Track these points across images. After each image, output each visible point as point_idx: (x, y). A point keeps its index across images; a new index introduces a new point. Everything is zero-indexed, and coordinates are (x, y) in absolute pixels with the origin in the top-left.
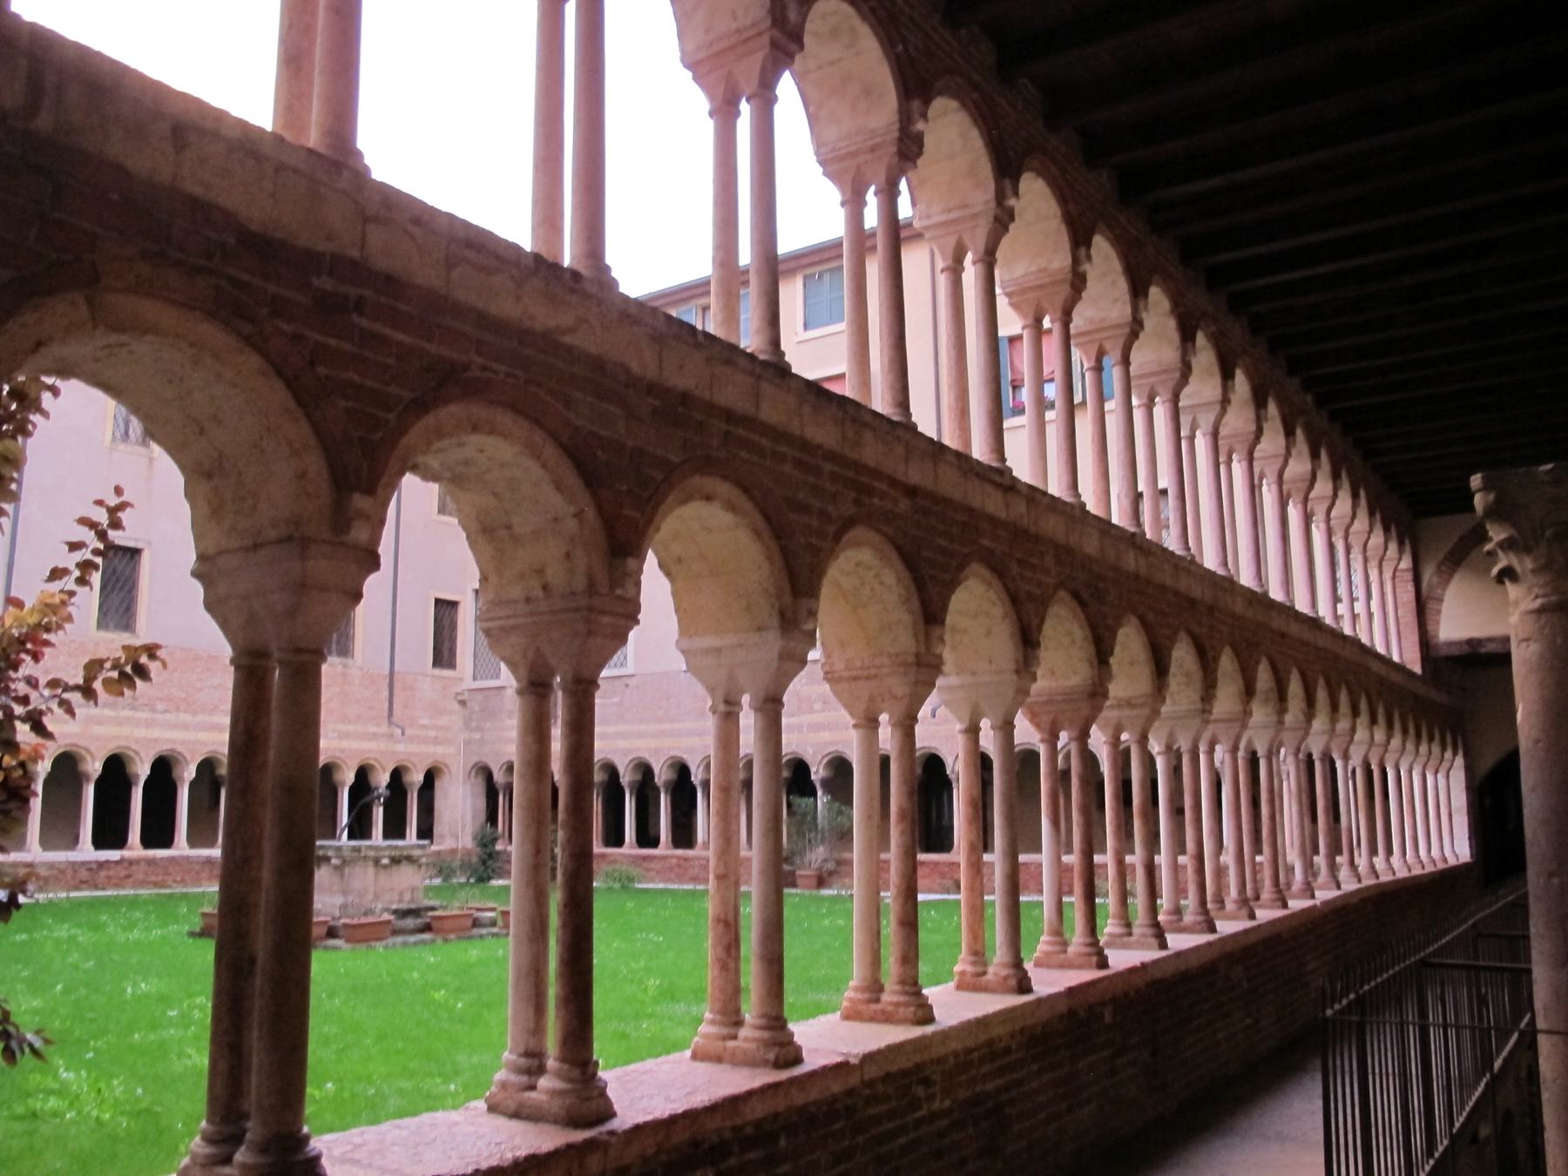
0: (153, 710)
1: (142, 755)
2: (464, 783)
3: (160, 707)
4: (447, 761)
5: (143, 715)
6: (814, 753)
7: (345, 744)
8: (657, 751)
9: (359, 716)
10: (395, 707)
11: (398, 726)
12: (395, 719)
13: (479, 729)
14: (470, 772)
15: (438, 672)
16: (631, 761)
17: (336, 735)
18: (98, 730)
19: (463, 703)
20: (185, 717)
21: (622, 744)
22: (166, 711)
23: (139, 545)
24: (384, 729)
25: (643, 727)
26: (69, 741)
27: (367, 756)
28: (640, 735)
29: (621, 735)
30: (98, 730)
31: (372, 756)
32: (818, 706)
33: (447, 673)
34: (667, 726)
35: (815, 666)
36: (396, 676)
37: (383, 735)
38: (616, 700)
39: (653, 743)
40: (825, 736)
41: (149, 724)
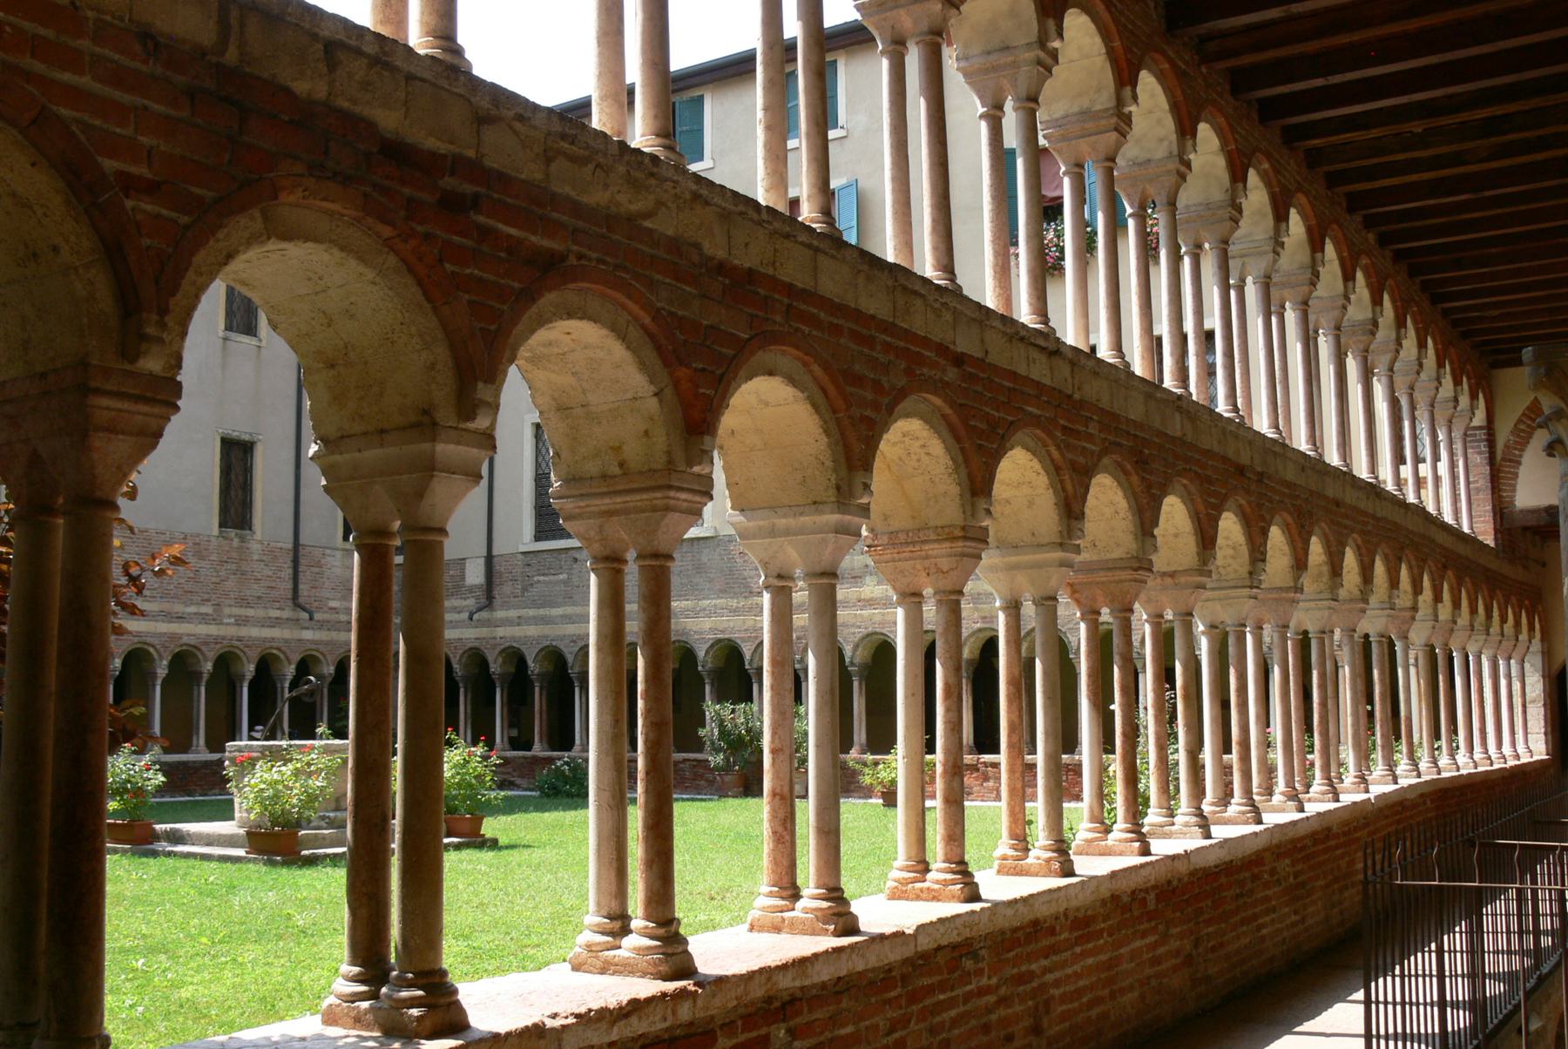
7: (245, 632)
9: (259, 598)
10: (301, 587)
11: (304, 609)
17: (233, 620)
24: (287, 614)
27: (268, 645)
31: (275, 645)
36: (302, 551)
38: (563, 577)
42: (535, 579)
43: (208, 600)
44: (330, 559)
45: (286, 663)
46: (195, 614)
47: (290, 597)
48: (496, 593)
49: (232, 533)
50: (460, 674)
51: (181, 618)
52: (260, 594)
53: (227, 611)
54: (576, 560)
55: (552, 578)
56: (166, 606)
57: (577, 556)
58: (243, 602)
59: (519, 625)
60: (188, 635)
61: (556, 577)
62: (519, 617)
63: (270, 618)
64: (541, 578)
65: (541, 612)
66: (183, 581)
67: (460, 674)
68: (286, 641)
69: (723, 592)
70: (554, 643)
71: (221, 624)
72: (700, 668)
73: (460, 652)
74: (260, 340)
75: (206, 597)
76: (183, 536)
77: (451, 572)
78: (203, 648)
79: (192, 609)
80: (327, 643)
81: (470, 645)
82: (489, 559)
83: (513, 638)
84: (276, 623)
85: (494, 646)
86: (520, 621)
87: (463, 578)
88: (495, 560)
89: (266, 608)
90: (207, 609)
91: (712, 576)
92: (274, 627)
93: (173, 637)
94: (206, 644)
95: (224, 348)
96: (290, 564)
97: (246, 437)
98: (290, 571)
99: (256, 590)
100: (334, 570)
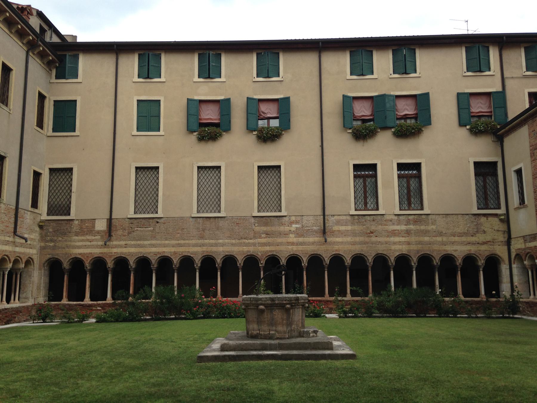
4: (33, 257)
6: (262, 255)
8: (175, 253)
12: (18, 233)
13: (51, 241)
14: (44, 264)
15: (32, 210)
16: (159, 258)
19: (41, 227)
21: (154, 250)
24: (11, 239)
25: (167, 242)
28: (165, 246)
29: (154, 246)
31: (6, 254)
32: (263, 236)
33: (36, 211)
34: (182, 242)
35: (262, 219)
37: (11, 242)
39: (173, 250)
40: (268, 248)
42: (136, 229)
44: (26, 215)
45: (8, 262)
47: (13, 231)
48: (113, 234)
50: (88, 268)
52: (3, 229)
54: (158, 222)
55: (145, 229)
57: (158, 221)
59: (125, 247)
61: (147, 229)
62: (125, 244)
63: (6, 241)
64: (139, 229)
65: (139, 242)
67: (88, 268)
68: (10, 252)
69: (230, 237)
70: (145, 255)
72: (217, 266)
73: (90, 259)
74: (10, 110)
77: (86, 225)
80: (23, 253)
81: (97, 256)
82: (110, 221)
83: (122, 253)
84: (7, 243)
85: (111, 256)
86: (126, 246)
87: (94, 226)
88: (113, 221)
89: (5, 236)
91: (224, 231)
92: (6, 245)
96: (14, 216)
98: (13, 219)
100: (27, 220)
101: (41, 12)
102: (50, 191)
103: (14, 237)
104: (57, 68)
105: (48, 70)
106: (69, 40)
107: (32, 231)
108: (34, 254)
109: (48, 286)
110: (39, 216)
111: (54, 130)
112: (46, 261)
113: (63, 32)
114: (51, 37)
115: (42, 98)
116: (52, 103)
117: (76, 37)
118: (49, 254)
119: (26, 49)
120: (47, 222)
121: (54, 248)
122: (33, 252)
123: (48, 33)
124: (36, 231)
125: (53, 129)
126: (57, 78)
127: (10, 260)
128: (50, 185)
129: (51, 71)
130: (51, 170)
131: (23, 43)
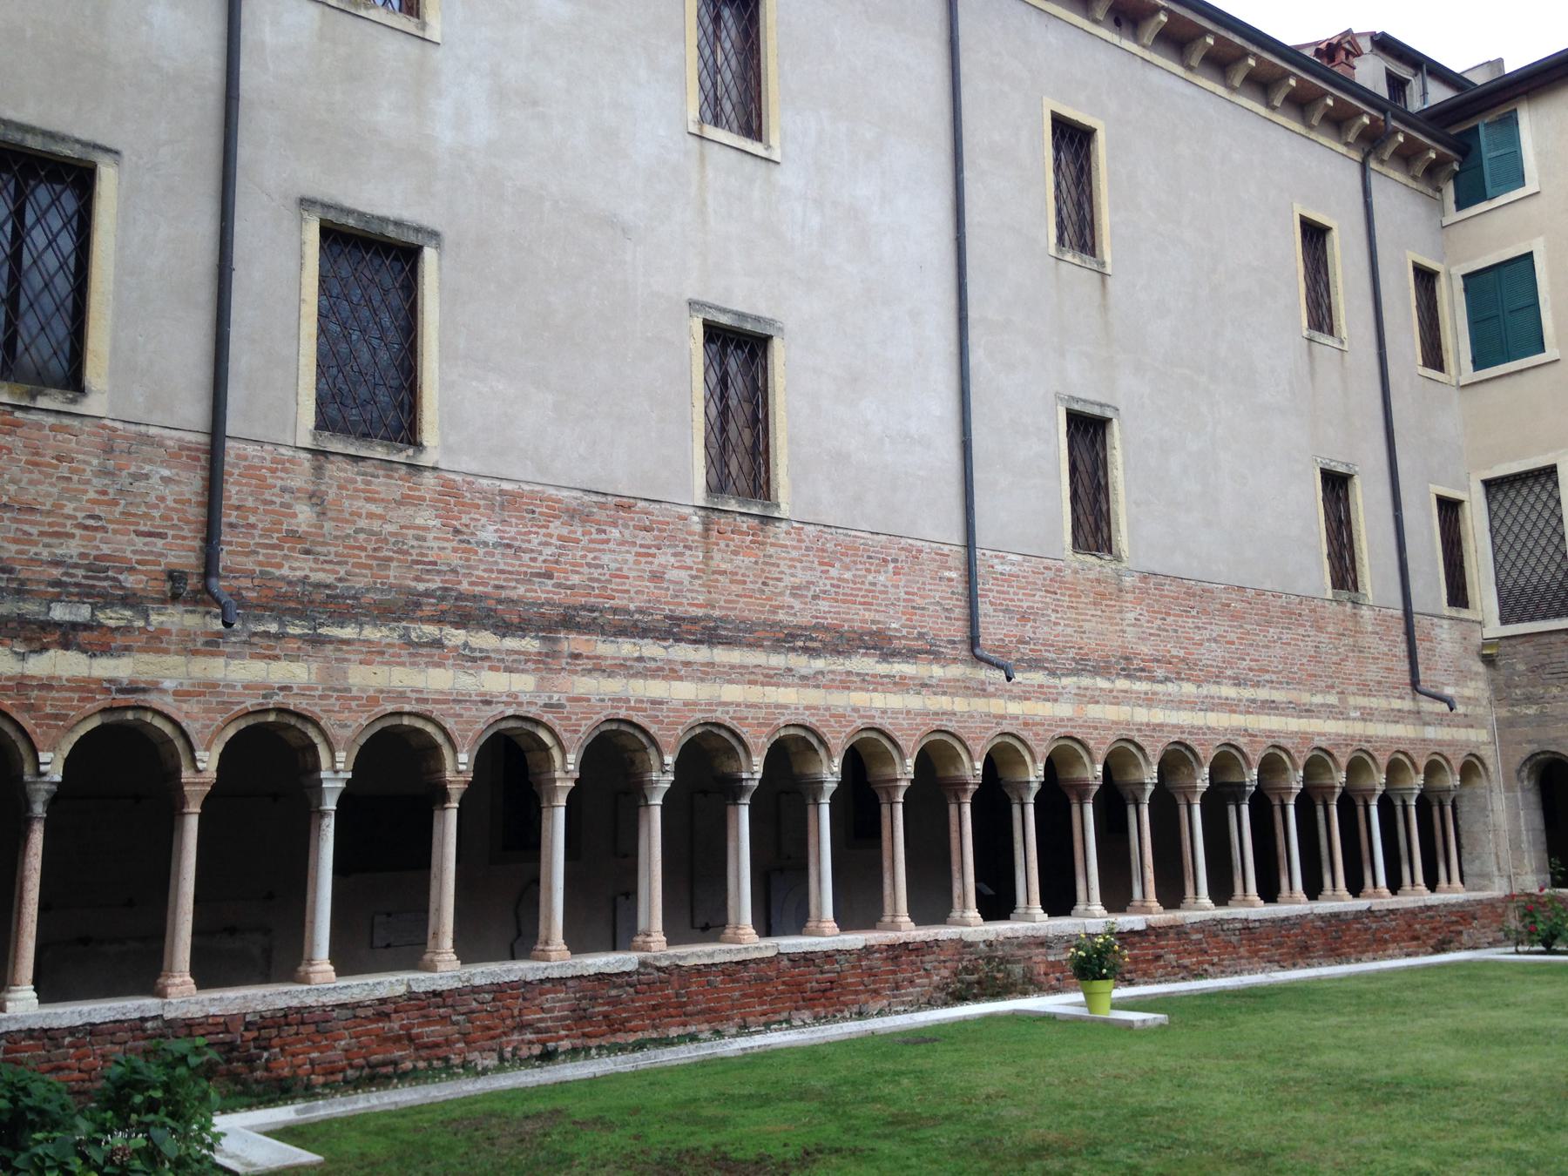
0: (1153, 680)
1: (1148, 751)
2: (1509, 788)
3: (1160, 673)
5: (1142, 686)
9: (1379, 683)
12: (1423, 686)
13: (1529, 699)
14: (1519, 772)
15: (1453, 612)
17: (1358, 714)
18: (1095, 711)
19: (1489, 661)
20: (1189, 688)
22: (1167, 679)
23: (1108, 414)
24: (1407, 704)
26: (1062, 731)
30: (1095, 711)
31: (1402, 747)
33: (1464, 614)
37: (1409, 712)
41: (1149, 701)
43: (1332, 687)
44: (1438, 630)
45: (1412, 772)
46: (1322, 705)
47: (1408, 681)
49: (1344, 594)
51: (1308, 712)
52: (1379, 678)
53: (1352, 700)
56: (1293, 695)
58: (1365, 689)
60: (1319, 734)
63: (1393, 710)
66: (1305, 661)
68: (1412, 741)
71: (1347, 719)
74: (1342, 342)
75: (1330, 681)
76: (1298, 600)
78: (1335, 752)
79: (1318, 699)
80: (1451, 743)
84: (1397, 717)
89: (1387, 696)
90: (1332, 699)
92: (1398, 722)
93: (1305, 737)
94: (1338, 746)
95: (1310, 353)
96: (1402, 638)
97: (1341, 469)
98: (1404, 646)
99: (1373, 673)
100: (1444, 644)
101: (1384, 35)
102: (1496, 550)
103: (1414, 699)
104: (1455, 176)
105: (1430, 192)
106: (1480, 79)
107: (1463, 676)
108: (1484, 743)
109: (1543, 838)
110: (1478, 627)
111: (1478, 364)
112: (1524, 763)
113: (1456, 63)
114: (1425, 94)
115: (1425, 278)
116: (1459, 284)
117: (1500, 61)
118: (1529, 742)
119: (1357, 156)
120: (1505, 642)
121: (1541, 720)
122: (1477, 737)
123: (1415, 86)
124: (1477, 674)
125: (1474, 362)
126: (1461, 204)
127: (1413, 764)
128: (1494, 532)
129: (1440, 190)
130: (1489, 484)
131: (1347, 144)
